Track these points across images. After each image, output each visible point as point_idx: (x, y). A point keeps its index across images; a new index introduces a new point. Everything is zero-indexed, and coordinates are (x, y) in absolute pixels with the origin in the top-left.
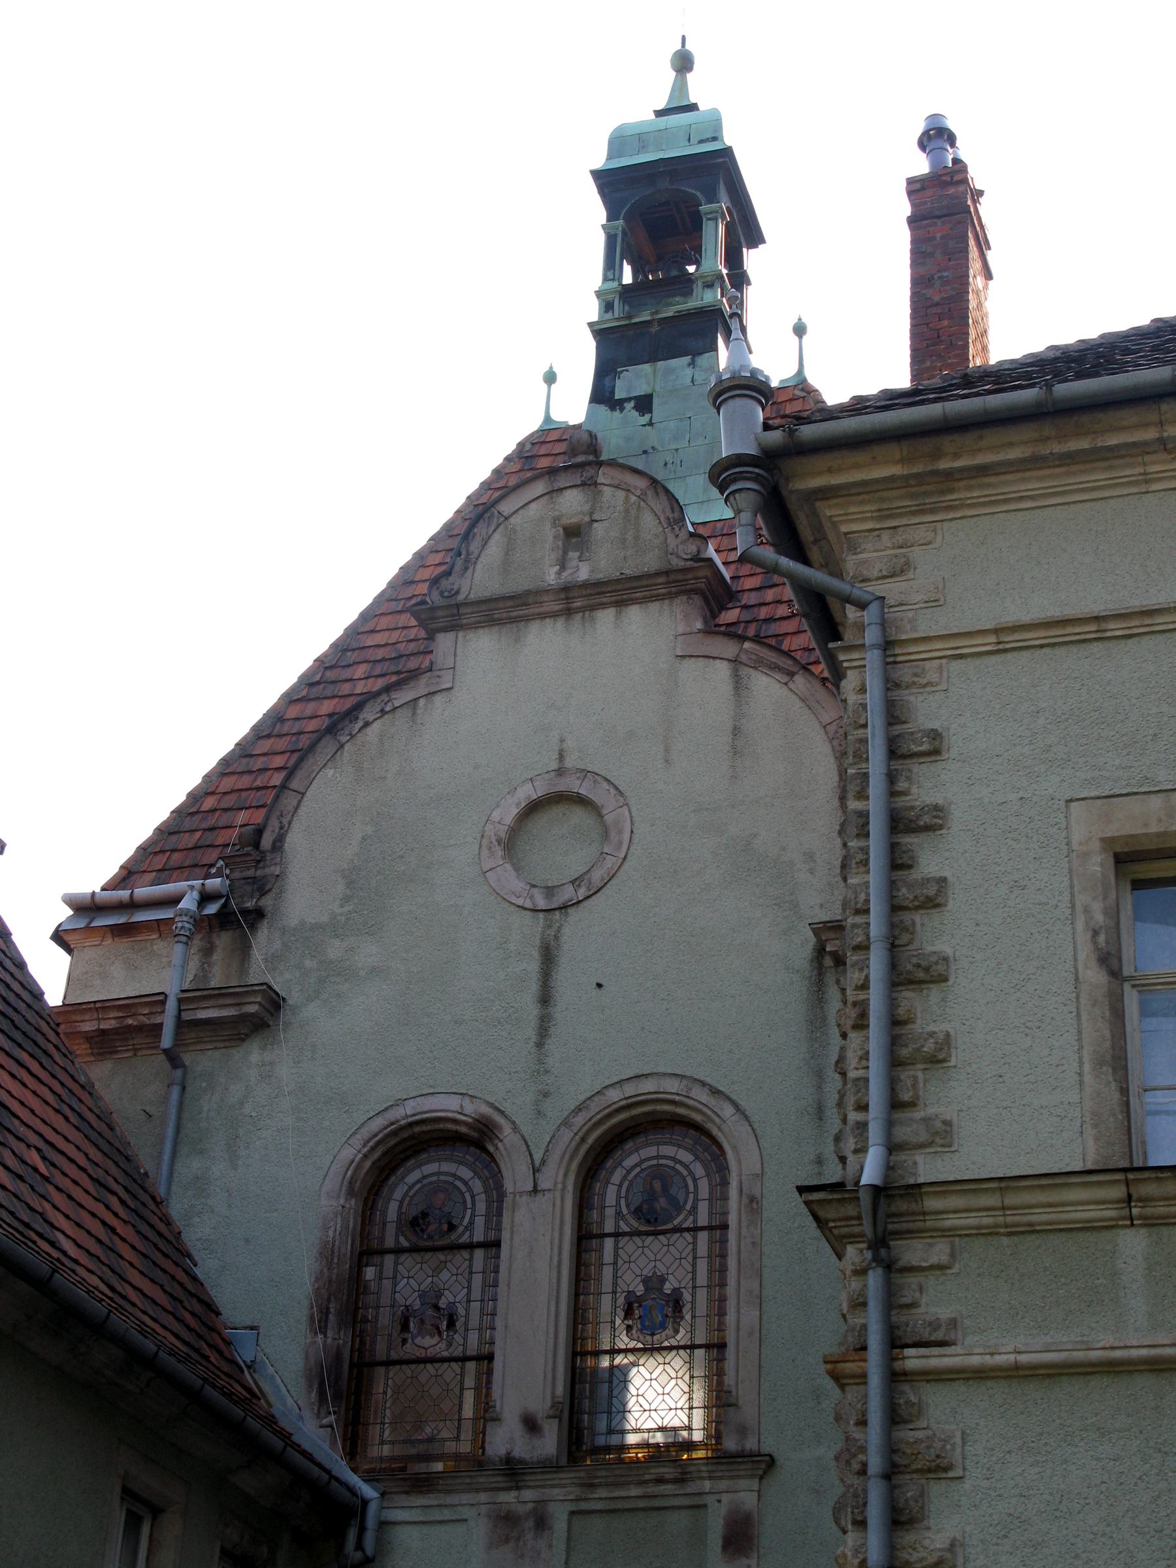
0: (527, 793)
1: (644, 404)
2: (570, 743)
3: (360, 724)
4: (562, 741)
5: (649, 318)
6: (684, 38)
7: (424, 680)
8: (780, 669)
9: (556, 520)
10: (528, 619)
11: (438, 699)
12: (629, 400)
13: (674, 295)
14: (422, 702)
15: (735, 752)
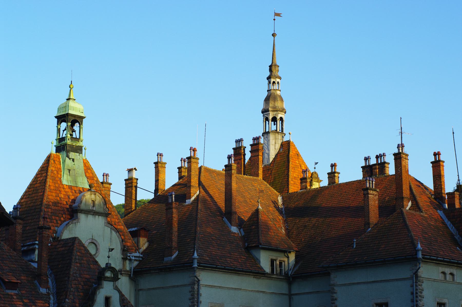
0: (89, 241)
1: (73, 160)
2: (93, 235)
3: (69, 224)
4: (92, 234)
5: (75, 145)
6: (71, 81)
7: (77, 220)
8: (116, 231)
9: (91, 199)
10: (89, 214)
11: (78, 223)
12: (71, 158)
13: (77, 141)
14: (76, 223)
15: (111, 242)
